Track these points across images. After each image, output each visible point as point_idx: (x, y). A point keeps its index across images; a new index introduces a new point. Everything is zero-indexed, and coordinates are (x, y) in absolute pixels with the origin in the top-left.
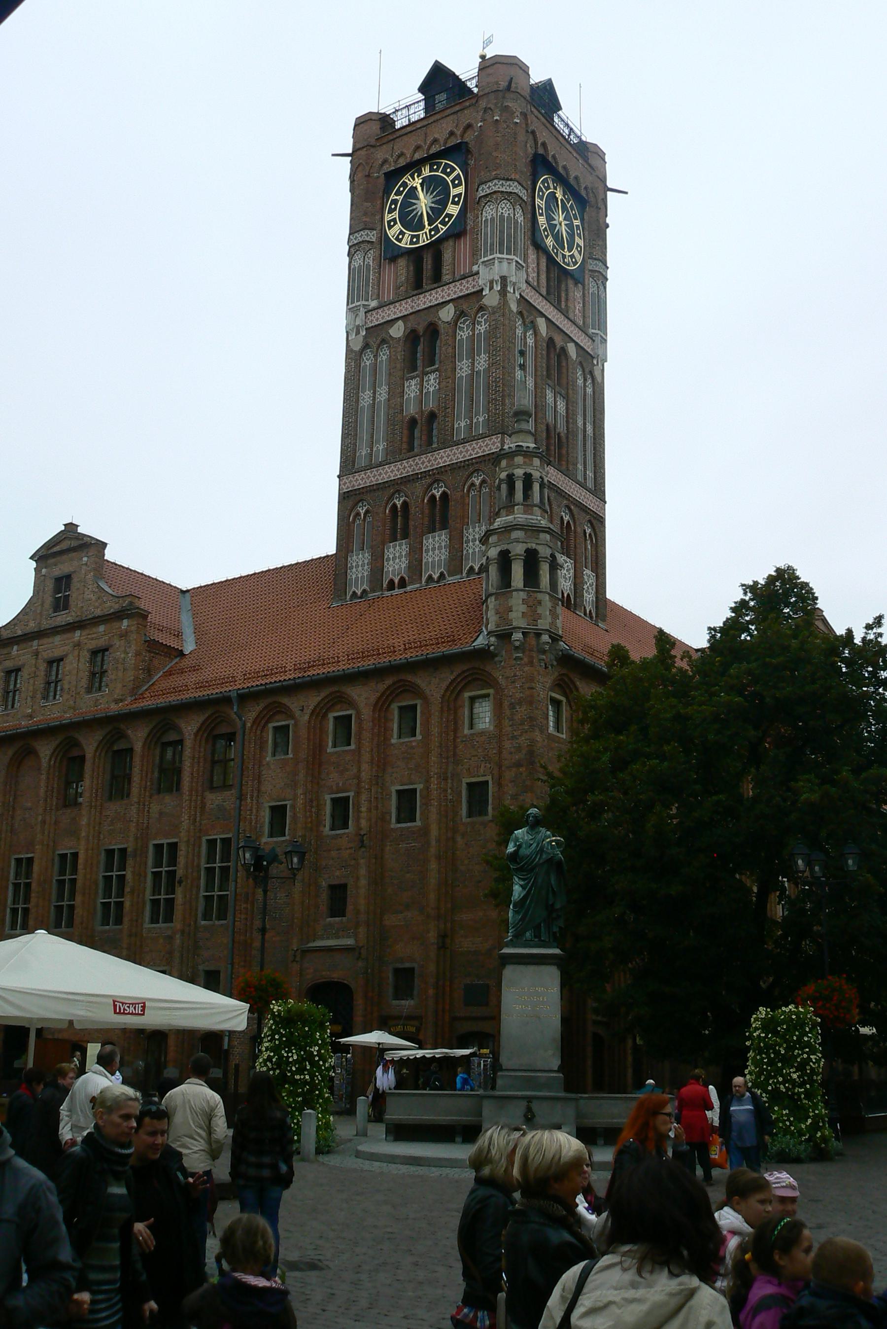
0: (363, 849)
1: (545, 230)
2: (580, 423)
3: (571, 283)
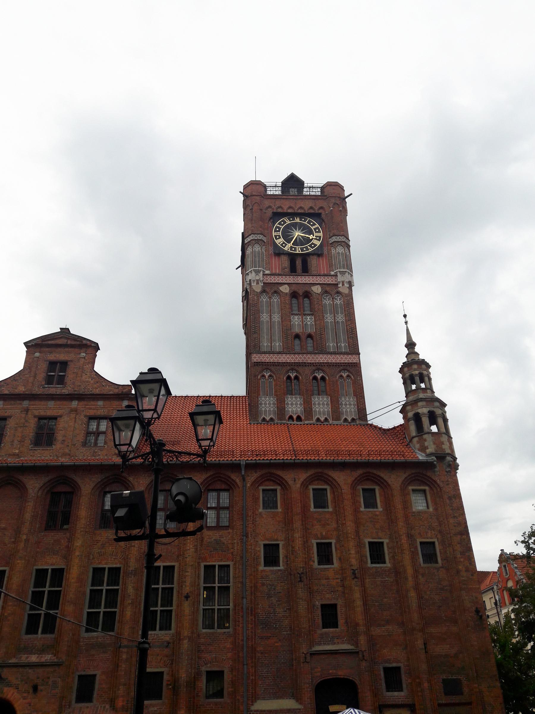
0: (356, 580)
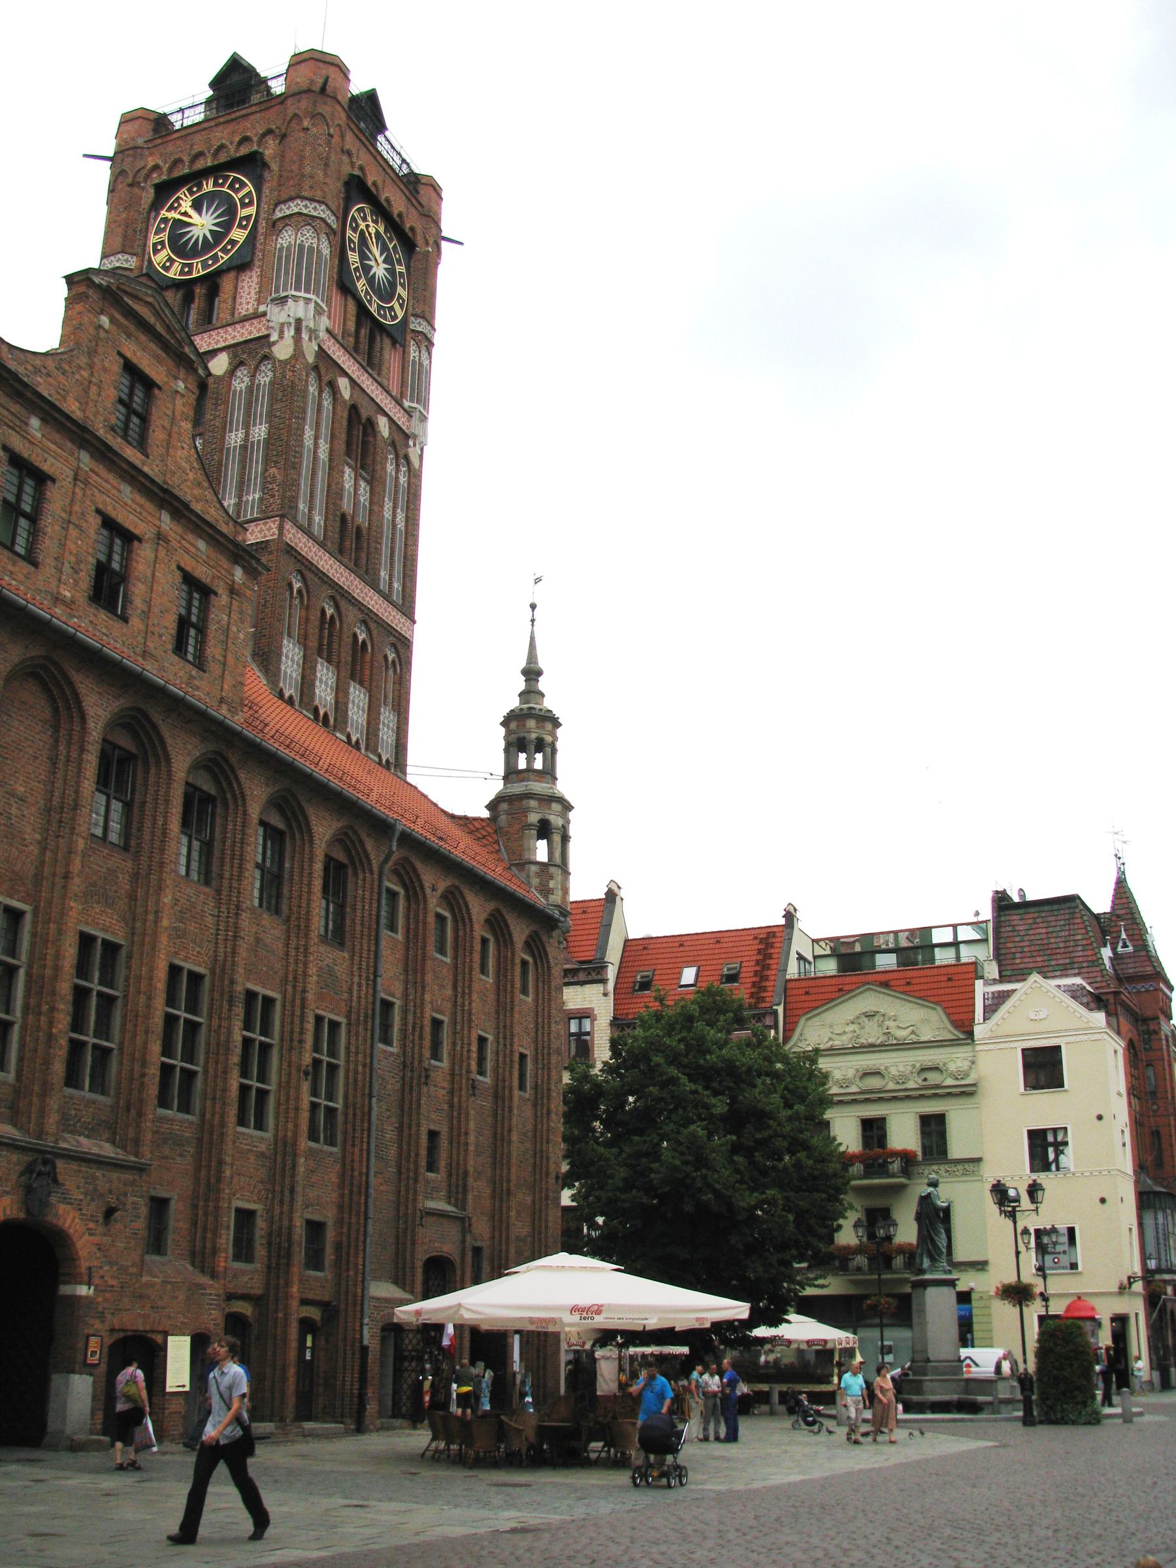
1: (356, 269)
3: (387, 342)
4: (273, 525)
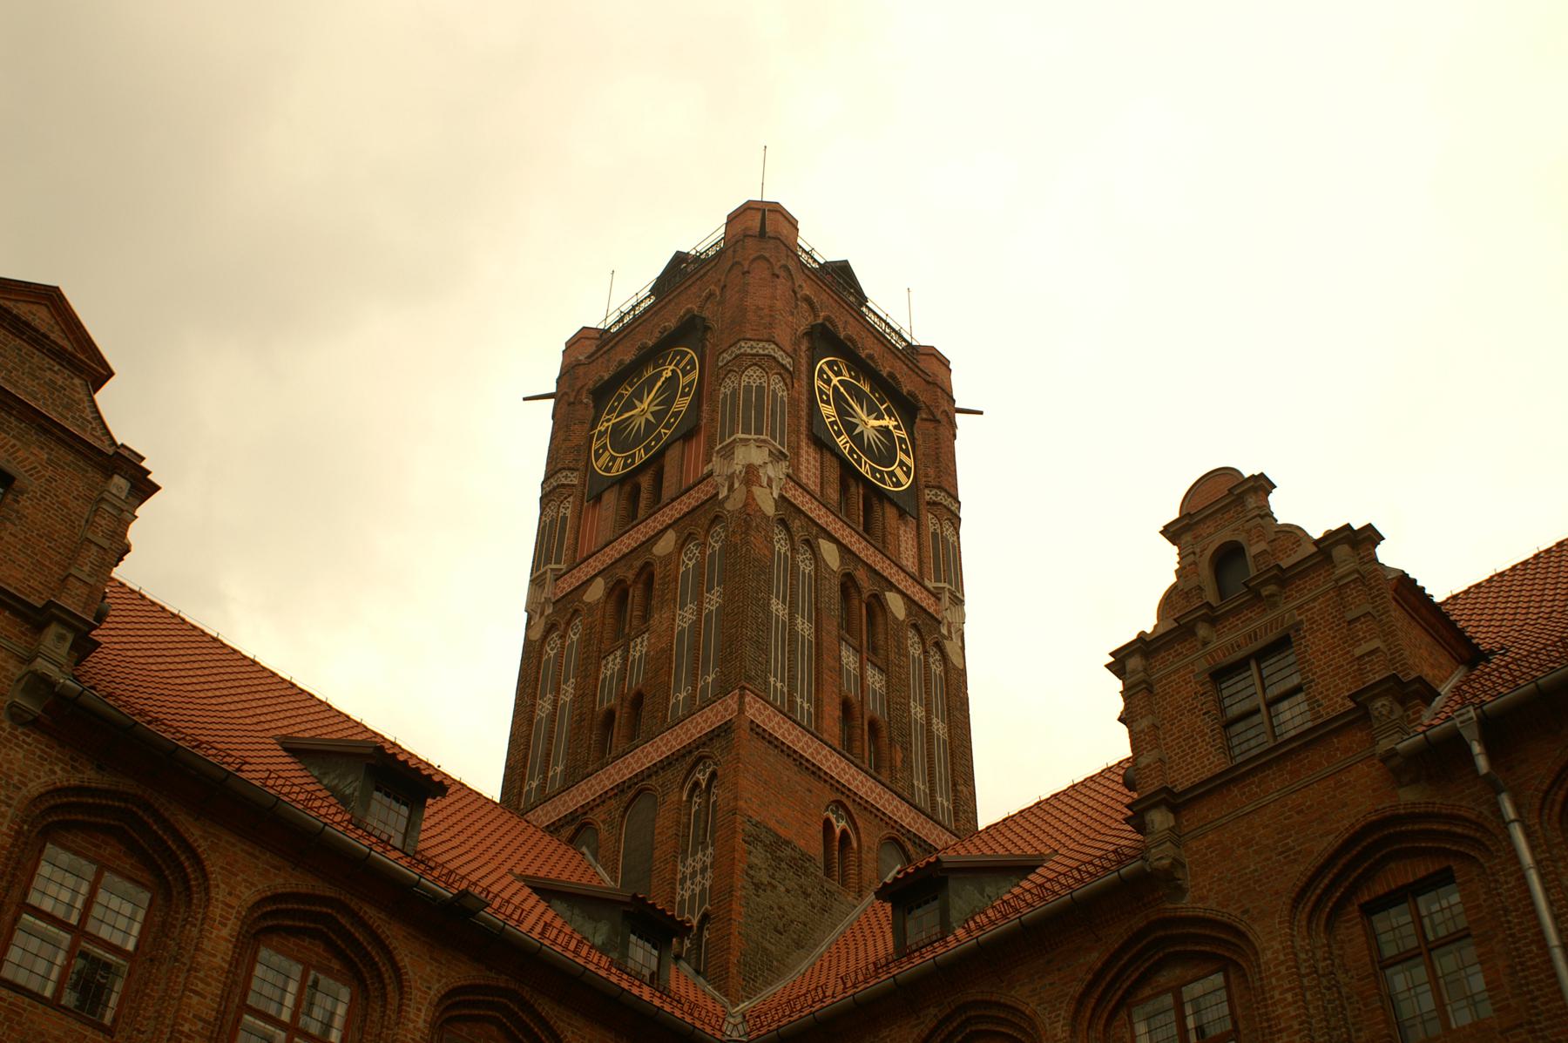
1: (835, 423)
2: (917, 711)
3: (891, 512)
4: (731, 702)
